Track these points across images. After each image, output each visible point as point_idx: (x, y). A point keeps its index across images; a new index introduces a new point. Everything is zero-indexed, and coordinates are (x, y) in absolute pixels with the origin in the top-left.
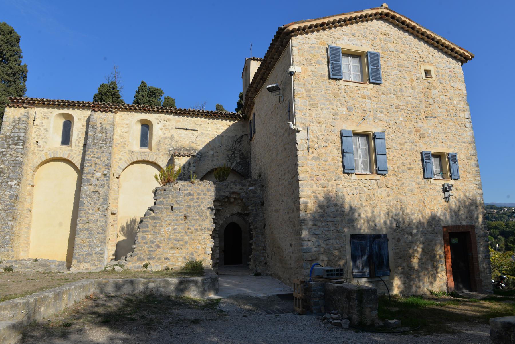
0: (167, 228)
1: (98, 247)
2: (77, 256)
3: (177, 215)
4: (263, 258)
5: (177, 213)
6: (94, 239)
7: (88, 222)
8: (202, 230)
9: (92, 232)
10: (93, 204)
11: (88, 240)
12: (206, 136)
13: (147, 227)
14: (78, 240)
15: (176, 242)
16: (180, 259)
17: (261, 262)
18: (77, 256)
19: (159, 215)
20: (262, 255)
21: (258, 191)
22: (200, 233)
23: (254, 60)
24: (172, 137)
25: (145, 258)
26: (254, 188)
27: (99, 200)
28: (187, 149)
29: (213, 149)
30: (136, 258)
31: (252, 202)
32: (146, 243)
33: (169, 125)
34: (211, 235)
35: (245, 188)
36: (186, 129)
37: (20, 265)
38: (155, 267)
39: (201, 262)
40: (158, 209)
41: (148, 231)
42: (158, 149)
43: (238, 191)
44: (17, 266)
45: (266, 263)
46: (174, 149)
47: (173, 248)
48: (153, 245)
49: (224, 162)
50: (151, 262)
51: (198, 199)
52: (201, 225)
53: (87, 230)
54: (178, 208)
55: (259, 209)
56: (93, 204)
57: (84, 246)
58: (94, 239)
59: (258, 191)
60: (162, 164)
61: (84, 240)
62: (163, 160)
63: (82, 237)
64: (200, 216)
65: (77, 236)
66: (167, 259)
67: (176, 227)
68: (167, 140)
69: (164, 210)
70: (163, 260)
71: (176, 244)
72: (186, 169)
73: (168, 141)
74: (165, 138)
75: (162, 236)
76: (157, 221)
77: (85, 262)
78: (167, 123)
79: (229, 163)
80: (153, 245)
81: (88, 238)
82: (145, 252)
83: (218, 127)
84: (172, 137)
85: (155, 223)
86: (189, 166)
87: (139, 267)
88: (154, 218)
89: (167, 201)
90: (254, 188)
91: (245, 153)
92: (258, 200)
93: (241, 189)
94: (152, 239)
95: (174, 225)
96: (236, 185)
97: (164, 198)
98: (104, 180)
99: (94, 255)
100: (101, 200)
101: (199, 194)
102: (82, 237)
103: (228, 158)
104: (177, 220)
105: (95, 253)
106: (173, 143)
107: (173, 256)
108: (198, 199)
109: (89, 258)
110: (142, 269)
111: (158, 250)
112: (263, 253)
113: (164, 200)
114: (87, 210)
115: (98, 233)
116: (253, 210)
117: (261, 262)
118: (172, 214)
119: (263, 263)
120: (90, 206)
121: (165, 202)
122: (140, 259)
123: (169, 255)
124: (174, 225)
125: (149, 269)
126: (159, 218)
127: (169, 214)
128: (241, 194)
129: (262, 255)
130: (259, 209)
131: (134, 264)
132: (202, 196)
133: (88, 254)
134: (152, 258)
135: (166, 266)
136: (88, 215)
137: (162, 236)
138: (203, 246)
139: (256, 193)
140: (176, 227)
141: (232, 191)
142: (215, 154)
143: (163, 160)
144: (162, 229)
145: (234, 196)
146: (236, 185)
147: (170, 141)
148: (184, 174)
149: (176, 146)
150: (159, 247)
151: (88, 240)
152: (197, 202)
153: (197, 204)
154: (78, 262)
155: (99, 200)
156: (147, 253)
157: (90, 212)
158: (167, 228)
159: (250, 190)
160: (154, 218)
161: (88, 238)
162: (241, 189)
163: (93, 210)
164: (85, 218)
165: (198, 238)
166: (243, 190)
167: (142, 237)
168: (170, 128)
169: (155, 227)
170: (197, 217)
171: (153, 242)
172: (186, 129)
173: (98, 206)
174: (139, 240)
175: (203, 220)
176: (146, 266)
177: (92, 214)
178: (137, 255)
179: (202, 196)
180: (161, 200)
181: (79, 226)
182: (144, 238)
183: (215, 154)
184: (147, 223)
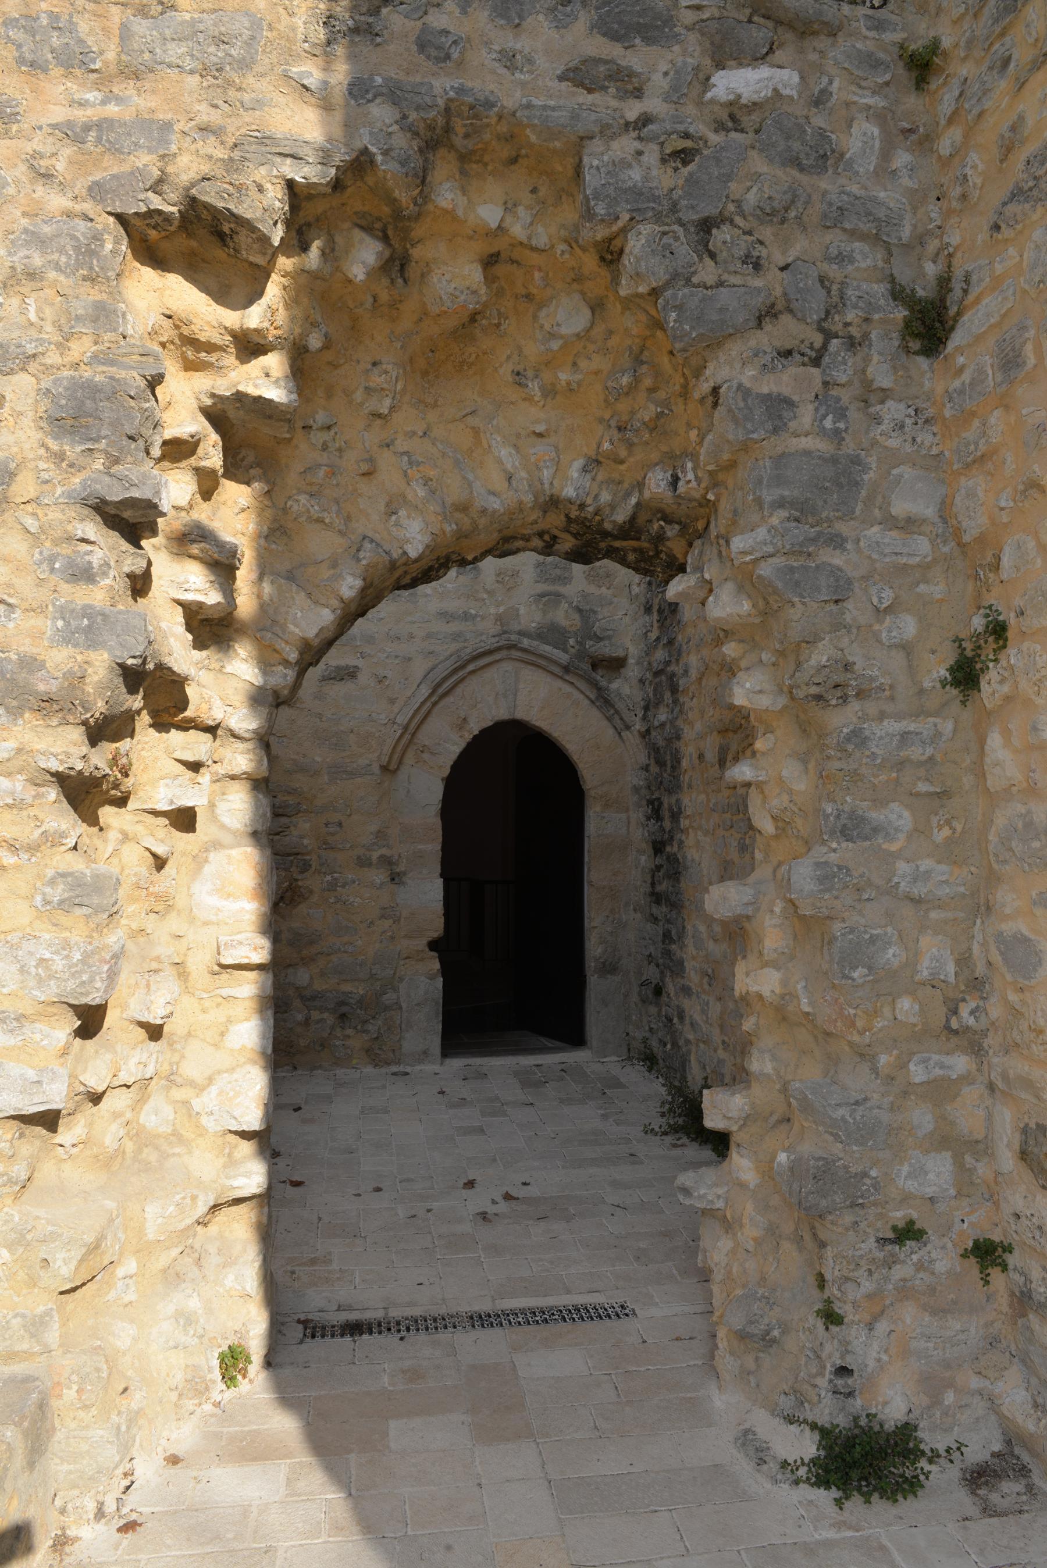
4: (938, 1172)
17: (908, 1233)
20: (922, 1118)
21: (861, 139)
26: (787, 79)
31: (771, 283)
45: (987, 1253)
55: (870, 395)
59: (861, 139)
90: (787, 79)
92: (866, 258)
93: (580, 76)
112: (942, 1091)
116: (778, 407)
117: (908, 1233)
119: (942, 1256)
128: (597, 158)
129: (922, 1118)
130: (870, 395)
139: (825, 157)
141: (442, 85)
145: (490, 214)
159: (733, 116)
162: (580, 76)
166: (632, 86)
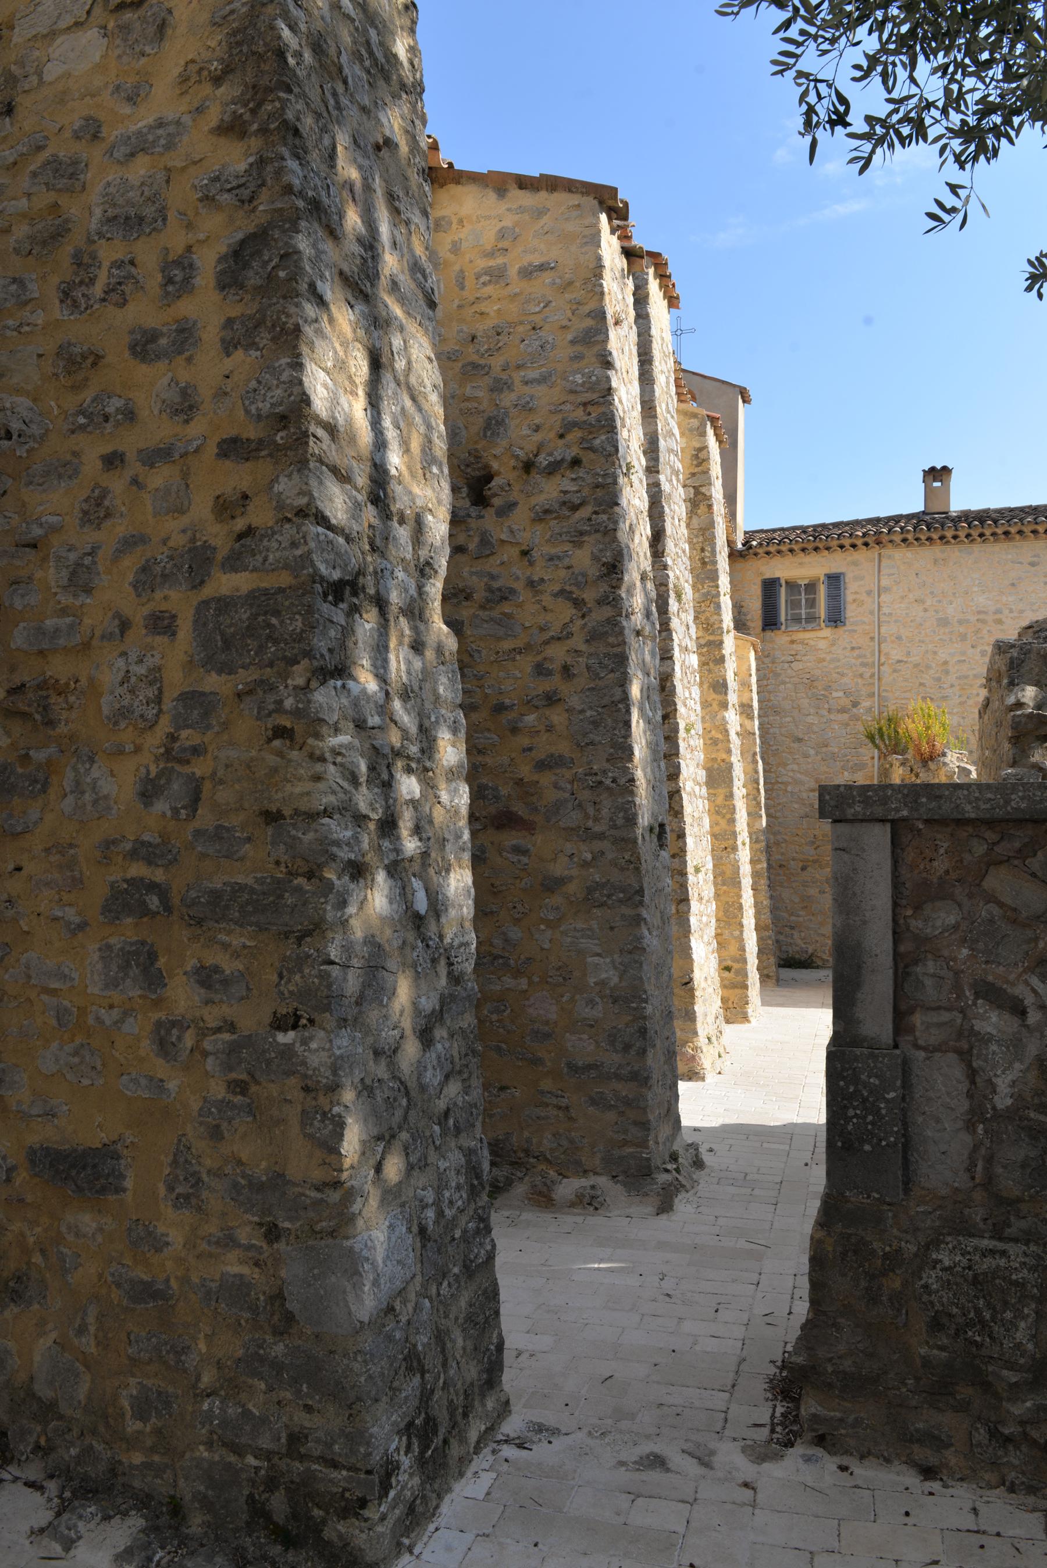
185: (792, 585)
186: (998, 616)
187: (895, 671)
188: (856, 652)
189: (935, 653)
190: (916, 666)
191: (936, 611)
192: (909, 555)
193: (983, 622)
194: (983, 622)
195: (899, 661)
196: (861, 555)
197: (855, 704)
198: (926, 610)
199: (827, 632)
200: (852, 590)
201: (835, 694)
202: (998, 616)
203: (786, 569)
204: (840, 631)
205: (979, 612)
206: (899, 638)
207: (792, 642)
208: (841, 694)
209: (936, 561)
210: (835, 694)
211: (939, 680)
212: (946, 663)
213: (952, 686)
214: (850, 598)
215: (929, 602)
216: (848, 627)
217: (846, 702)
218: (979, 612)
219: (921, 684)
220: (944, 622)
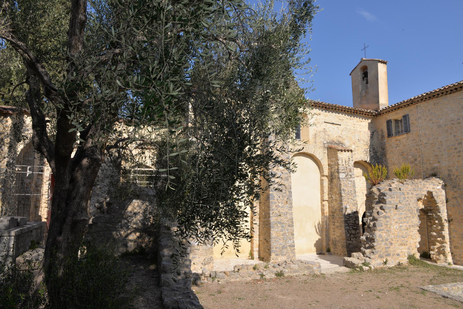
0: (395, 226)
1: (290, 239)
2: (274, 249)
3: (401, 214)
5: (401, 212)
6: (287, 232)
7: (280, 215)
8: (413, 226)
9: (284, 225)
10: (281, 198)
11: (282, 233)
12: (349, 131)
13: (382, 226)
14: (274, 233)
15: (403, 239)
16: (406, 254)
18: (274, 249)
19: (388, 215)
22: (412, 228)
23: (381, 62)
24: (325, 131)
25: (384, 255)
27: (286, 193)
28: (336, 143)
29: (354, 144)
30: (377, 255)
32: (382, 241)
33: (320, 119)
34: (418, 231)
35: (435, 187)
36: (333, 124)
37: (289, 269)
38: (392, 263)
39: (414, 254)
40: (389, 208)
41: (383, 230)
42: (316, 143)
43: (431, 190)
44: (287, 270)
46: (328, 143)
47: (401, 245)
48: (387, 242)
49: (362, 155)
50: (388, 258)
51: (408, 198)
52: (412, 222)
53: (280, 223)
54: (401, 207)
56: (281, 198)
57: (279, 239)
58: (287, 232)
60: (320, 157)
61: (278, 232)
62: (319, 153)
63: (276, 230)
64: (411, 213)
65: (272, 229)
66: (398, 255)
67: (401, 225)
68: (321, 133)
69: (392, 209)
70: (396, 256)
71: (403, 241)
72: (347, 163)
73: (322, 134)
74: (320, 132)
75: (393, 234)
76: (388, 219)
77: (282, 255)
78: (318, 117)
79: (366, 157)
80: (387, 242)
81: (281, 231)
82: (383, 249)
83: (355, 123)
84: (325, 131)
85: (387, 221)
86: (349, 160)
87: (380, 264)
88: (385, 217)
89: (394, 201)
91: (375, 148)
94: (386, 237)
95: (400, 223)
96: (430, 185)
97: (392, 198)
98: (287, 173)
99: (288, 248)
100: (288, 193)
101: (408, 193)
102: (276, 230)
103: (365, 152)
104: (401, 218)
105: (289, 246)
106: (327, 137)
107: (402, 252)
108: (408, 198)
109: (285, 251)
110: (382, 266)
111: (392, 247)
113: (392, 200)
114: (277, 204)
115: (289, 226)
118: (397, 213)
120: (279, 199)
121: (392, 202)
122: (381, 257)
123: (398, 251)
124: (400, 223)
125: (388, 265)
126: (389, 217)
127: (396, 213)
131: (377, 262)
132: (410, 195)
133: (283, 247)
134: (388, 255)
135: (397, 261)
136: (279, 208)
137: (393, 234)
138: (415, 241)
140: (401, 225)
142: (356, 148)
143: (319, 153)
144: (392, 228)
146: (430, 185)
147: (324, 134)
148: (346, 167)
149: (328, 139)
150: (391, 244)
151: (282, 233)
152: (407, 201)
153: (408, 203)
154: (277, 255)
155: (286, 193)
156: (384, 250)
157: (280, 205)
158: (395, 226)
160: (385, 217)
161: (281, 231)
163: (282, 203)
164: (277, 212)
165: (411, 234)
167: (379, 236)
168: (321, 122)
169: (387, 225)
170: (410, 215)
171: (387, 240)
172: (333, 124)
173: (286, 199)
174: (377, 238)
175: (414, 217)
176: (385, 263)
177: (282, 207)
178: (378, 252)
179: (410, 195)
180: (390, 200)
181: (273, 219)
182: (380, 236)
183: (356, 148)
184: (382, 222)
185: (396, 121)
186: (459, 121)
187: (425, 147)
188: (414, 141)
189: (437, 138)
190: (432, 144)
191: (437, 123)
192: (426, 104)
193: (453, 124)
194: (453, 124)
195: (426, 143)
196: (412, 107)
197: (416, 160)
198: (433, 123)
199: (405, 136)
200: (412, 119)
201: (409, 157)
202: (459, 121)
203: (393, 116)
204: (409, 134)
205: (451, 121)
206: (425, 134)
207: (397, 140)
208: (411, 157)
209: (434, 104)
210: (409, 157)
211: (439, 148)
212: (441, 142)
213: (444, 150)
214: (411, 123)
215: (434, 120)
216: (411, 133)
217: (413, 159)
218: (451, 121)
219: (434, 151)
220: (439, 126)
